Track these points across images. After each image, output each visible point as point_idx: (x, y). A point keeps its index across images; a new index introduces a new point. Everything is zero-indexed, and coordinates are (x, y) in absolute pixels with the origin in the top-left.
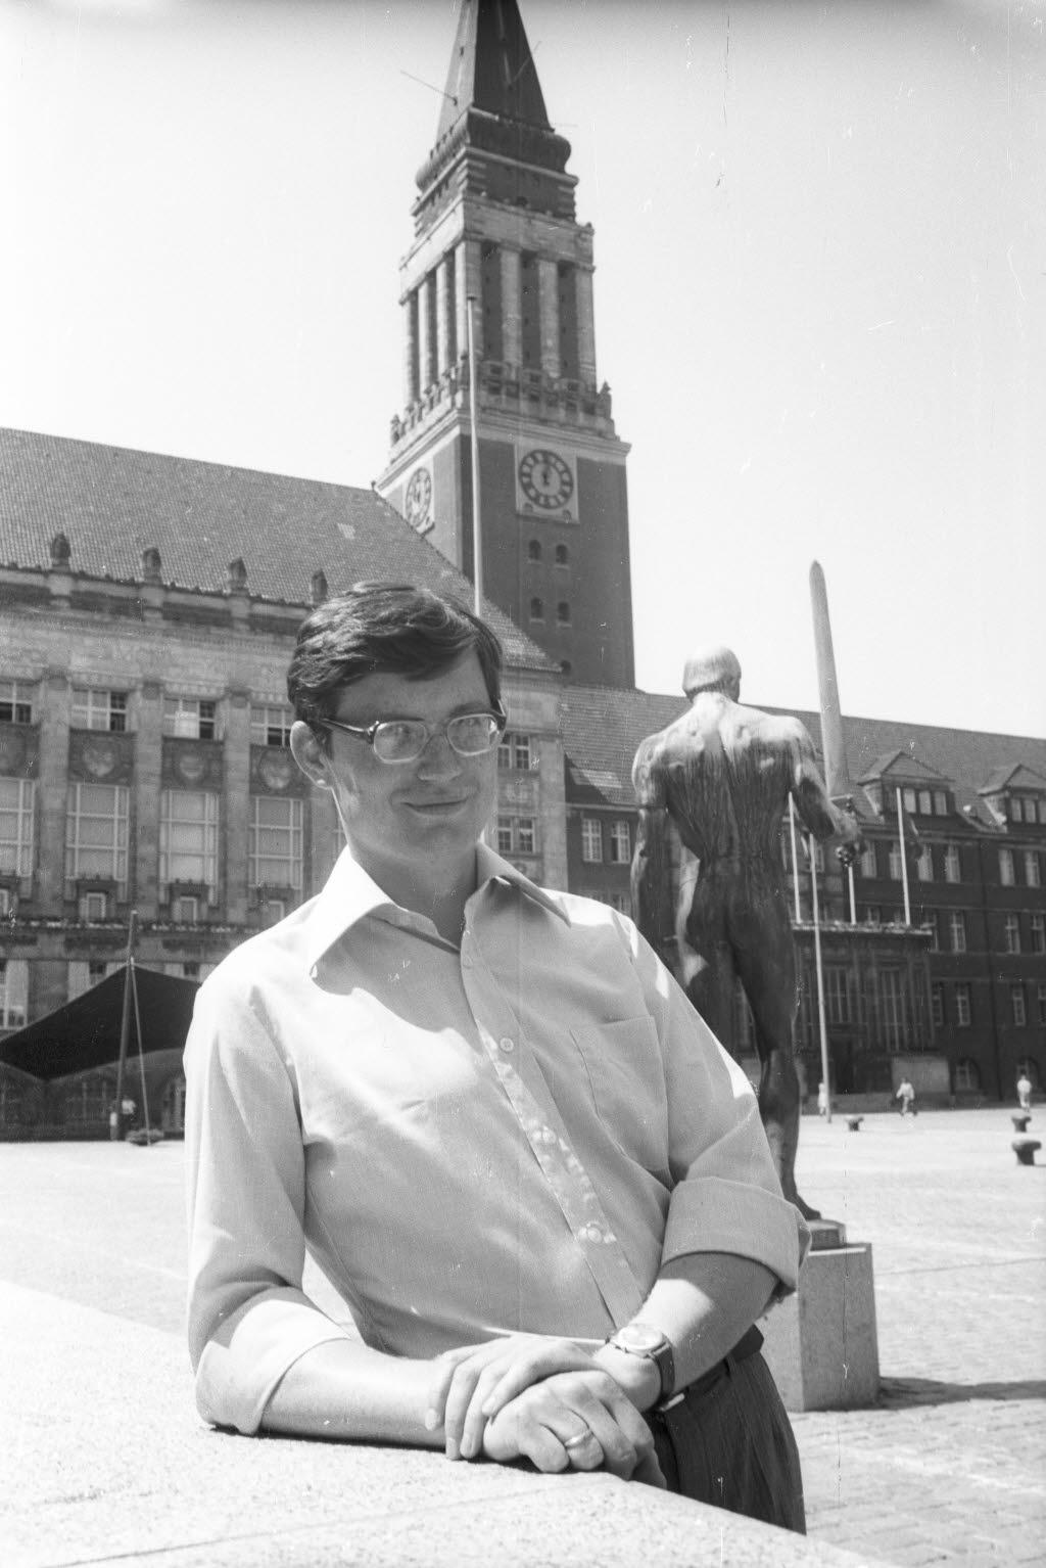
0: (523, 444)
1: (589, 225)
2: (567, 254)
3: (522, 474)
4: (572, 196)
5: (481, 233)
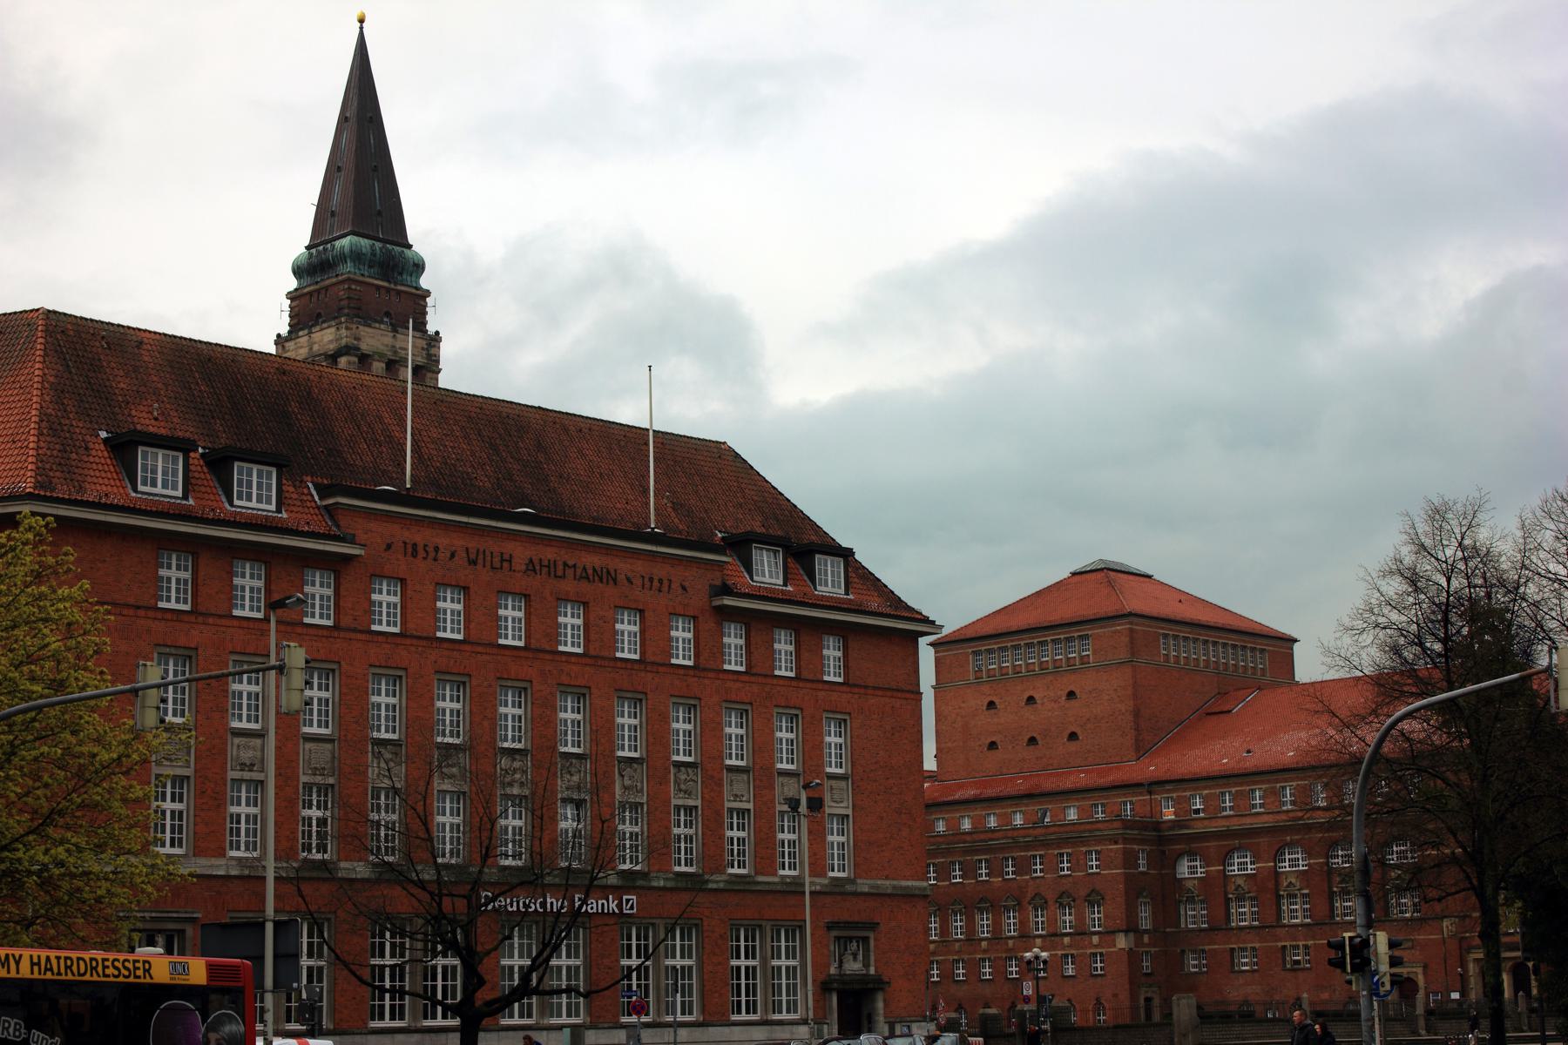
1: (437, 333)
4: (425, 306)
5: (359, 349)
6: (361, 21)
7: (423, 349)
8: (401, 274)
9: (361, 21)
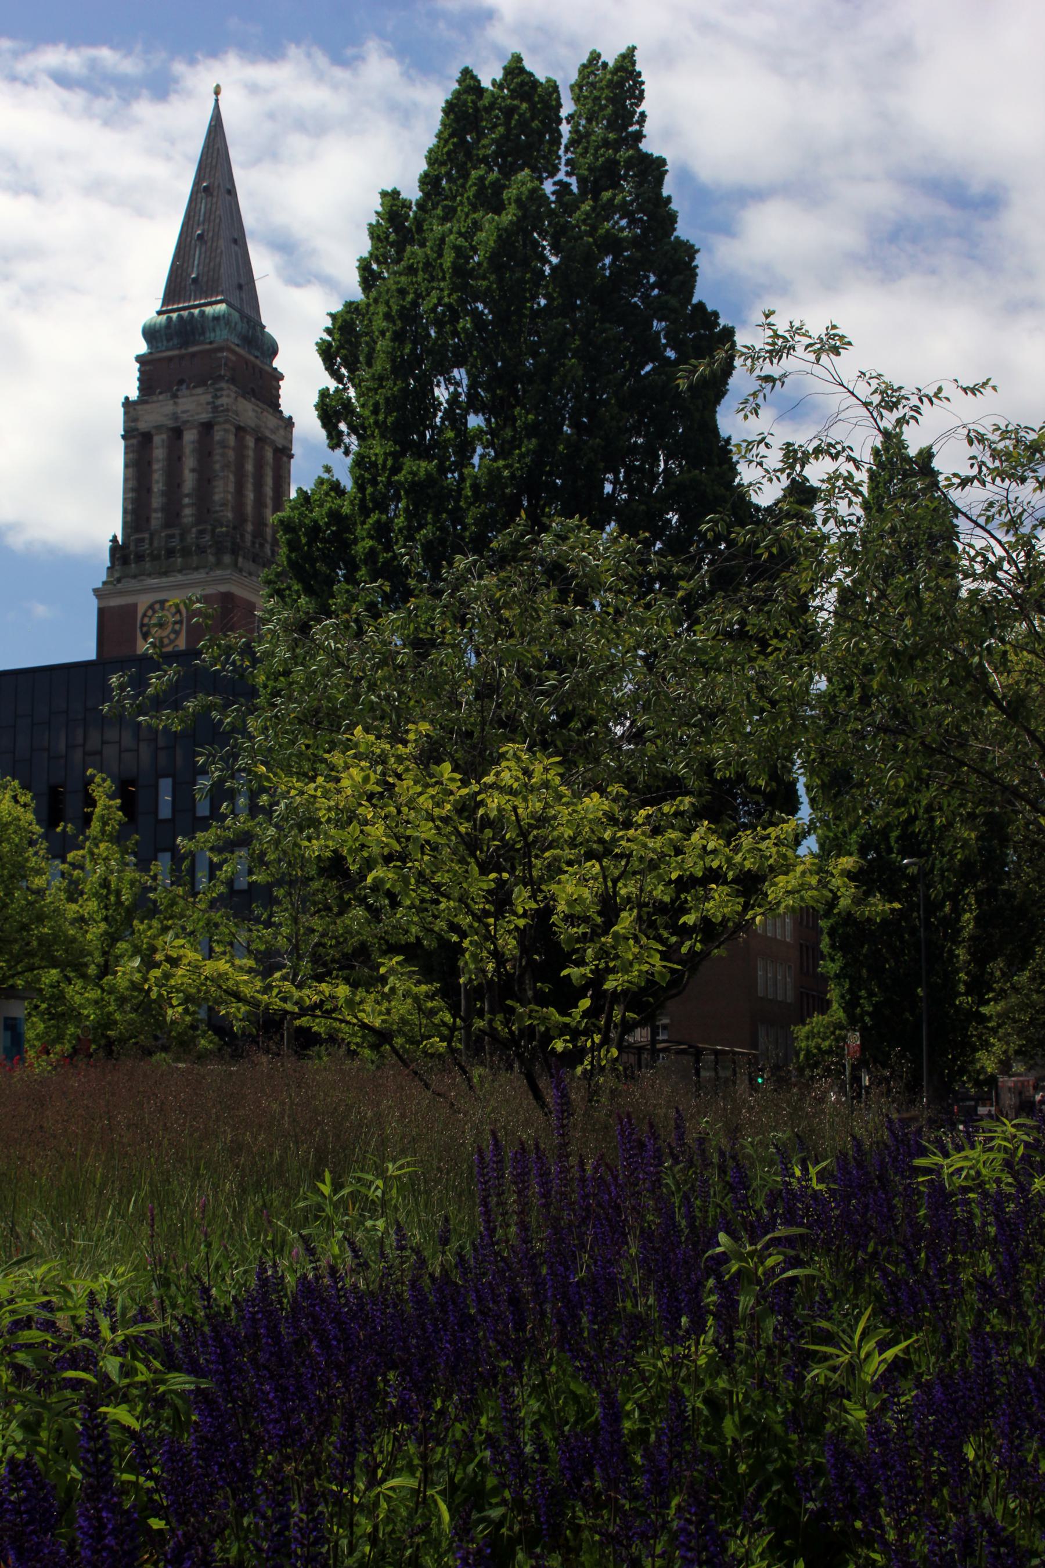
0: (143, 602)
2: (204, 417)
3: (143, 625)
6: (217, 91)
7: (208, 403)
8: (203, 333)
9: (217, 91)
